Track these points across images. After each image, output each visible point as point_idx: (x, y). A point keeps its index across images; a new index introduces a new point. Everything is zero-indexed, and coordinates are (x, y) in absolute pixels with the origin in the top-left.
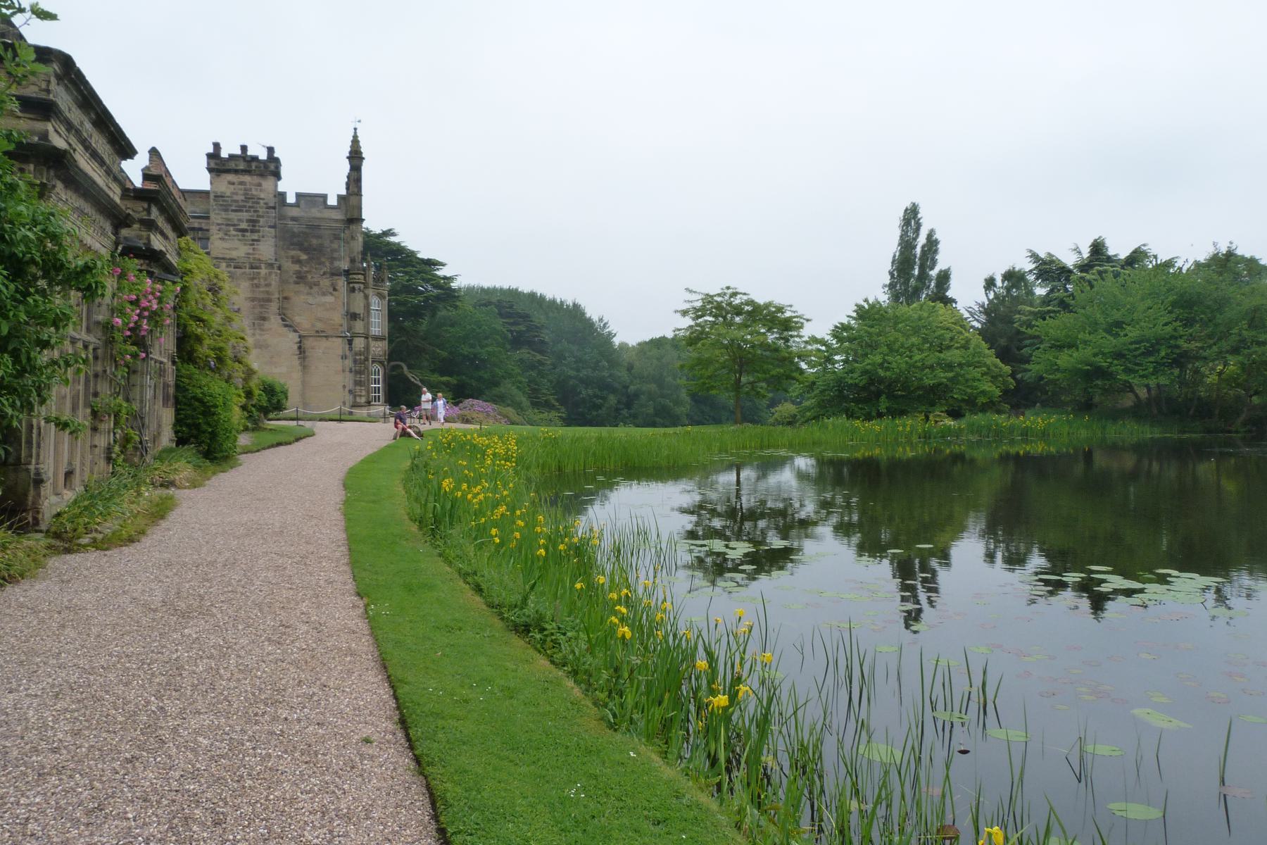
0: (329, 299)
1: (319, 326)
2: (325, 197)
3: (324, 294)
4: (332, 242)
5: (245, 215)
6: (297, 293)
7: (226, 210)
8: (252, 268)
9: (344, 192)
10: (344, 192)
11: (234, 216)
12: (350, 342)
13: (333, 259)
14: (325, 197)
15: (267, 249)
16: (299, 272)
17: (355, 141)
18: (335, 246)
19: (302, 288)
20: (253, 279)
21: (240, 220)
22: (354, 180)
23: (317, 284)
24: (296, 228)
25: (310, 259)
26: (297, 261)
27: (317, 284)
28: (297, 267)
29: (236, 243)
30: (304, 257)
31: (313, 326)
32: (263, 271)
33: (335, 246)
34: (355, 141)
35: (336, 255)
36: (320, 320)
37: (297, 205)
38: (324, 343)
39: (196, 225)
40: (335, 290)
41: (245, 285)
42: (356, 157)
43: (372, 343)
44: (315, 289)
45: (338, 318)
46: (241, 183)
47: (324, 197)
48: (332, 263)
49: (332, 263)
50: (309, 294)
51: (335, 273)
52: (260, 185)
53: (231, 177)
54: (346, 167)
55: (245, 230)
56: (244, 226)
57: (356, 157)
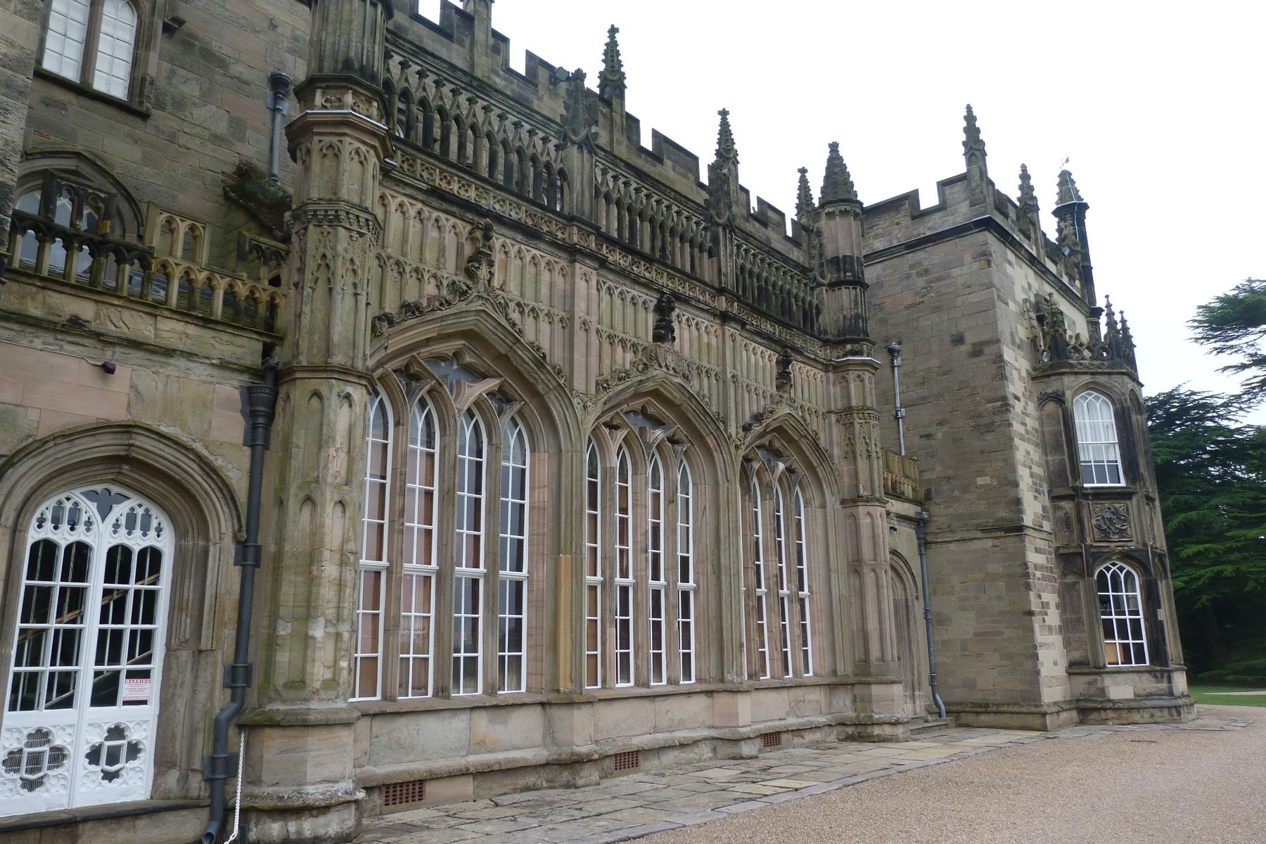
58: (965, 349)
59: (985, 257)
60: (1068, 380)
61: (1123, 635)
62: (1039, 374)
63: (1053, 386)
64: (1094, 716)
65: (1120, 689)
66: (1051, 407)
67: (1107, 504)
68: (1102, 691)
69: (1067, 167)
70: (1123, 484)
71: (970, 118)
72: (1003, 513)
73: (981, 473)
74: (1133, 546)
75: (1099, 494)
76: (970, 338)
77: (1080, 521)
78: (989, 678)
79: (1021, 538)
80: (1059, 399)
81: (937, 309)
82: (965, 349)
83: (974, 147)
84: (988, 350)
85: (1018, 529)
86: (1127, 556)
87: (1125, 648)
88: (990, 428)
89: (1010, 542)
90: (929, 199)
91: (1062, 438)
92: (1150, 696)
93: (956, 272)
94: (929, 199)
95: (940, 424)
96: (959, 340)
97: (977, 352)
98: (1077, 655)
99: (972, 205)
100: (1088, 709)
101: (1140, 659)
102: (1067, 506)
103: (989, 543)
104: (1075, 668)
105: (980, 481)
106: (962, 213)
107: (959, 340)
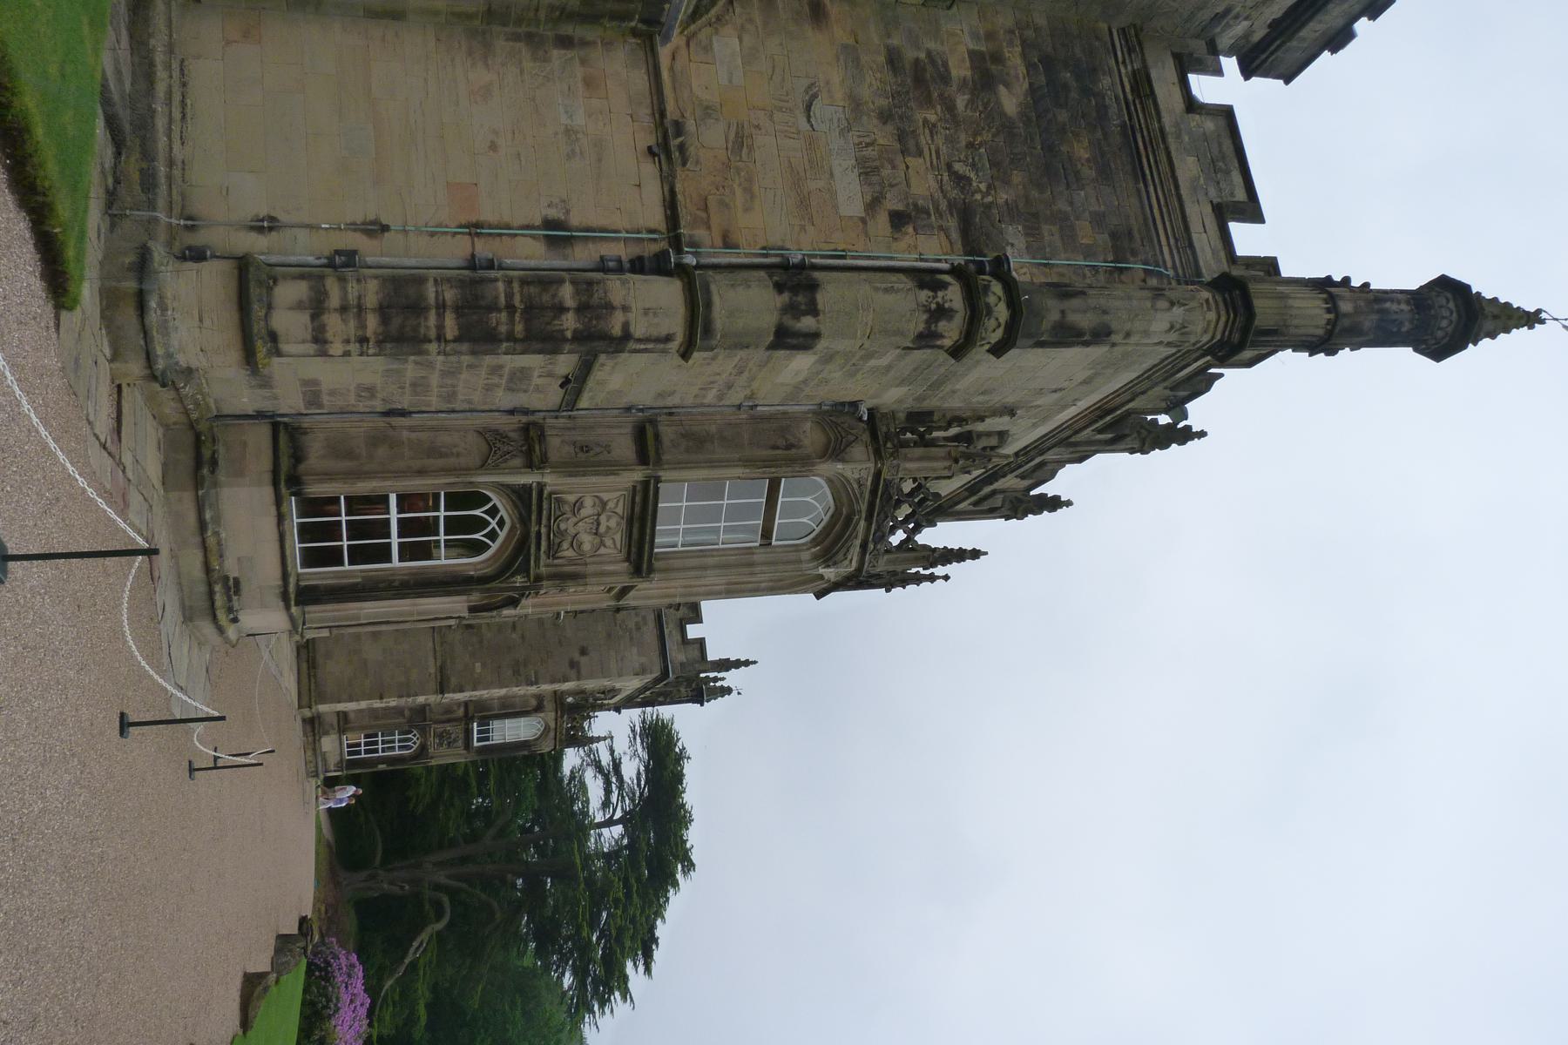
0: (850, 195)
1: (709, 140)
2: (1252, 212)
3: (867, 171)
4: (1098, 220)
6: (850, 55)
12: (658, 266)
13: (1032, 222)
14: (1252, 212)
16: (945, 78)
18: (1085, 233)
19: (874, 85)
22: (1346, 317)
23: (906, 142)
24: (1112, 83)
25: (1007, 127)
26: (986, 73)
27: (906, 142)
28: (960, 69)
30: (1010, 102)
31: (708, 111)
33: (1085, 233)
35: (1050, 232)
36: (740, 141)
37: (1192, 105)
38: (627, 137)
40: (899, 220)
43: (615, 489)
44: (884, 136)
45: (767, 223)
48: (1012, 212)
49: (1012, 212)
50: (856, 104)
51: (970, 224)
58: (576, 656)
59: (642, 671)
60: (552, 715)
61: (366, 744)
62: (558, 697)
63: (549, 704)
64: (309, 728)
65: (328, 744)
66: (534, 702)
67: (462, 736)
68: (326, 733)
69: (735, 693)
70: (476, 744)
71: (747, 663)
72: (454, 681)
73: (484, 665)
74: (431, 750)
75: (468, 733)
76: (583, 660)
77: (449, 721)
78: (334, 669)
79: (436, 693)
80: (539, 708)
81: (609, 635)
82: (576, 656)
83: (726, 665)
84: (573, 673)
85: (442, 690)
86: (423, 748)
87: (359, 745)
88: (516, 672)
89: (433, 685)
90: (693, 631)
91: (511, 710)
92: (325, 760)
93: (635, 650)
94: (693, 631)
95: (523, 637)
96: (583, 652)
97: (573, 665)
98: (352, 716)
99: (682, 664)
100: (314, 726)
101: (350, 753)
102: (461, 712)
103: (432, 671)
104: (343, 717)
105: (478, 665)
106: (677, 655)
107: (583, 652)
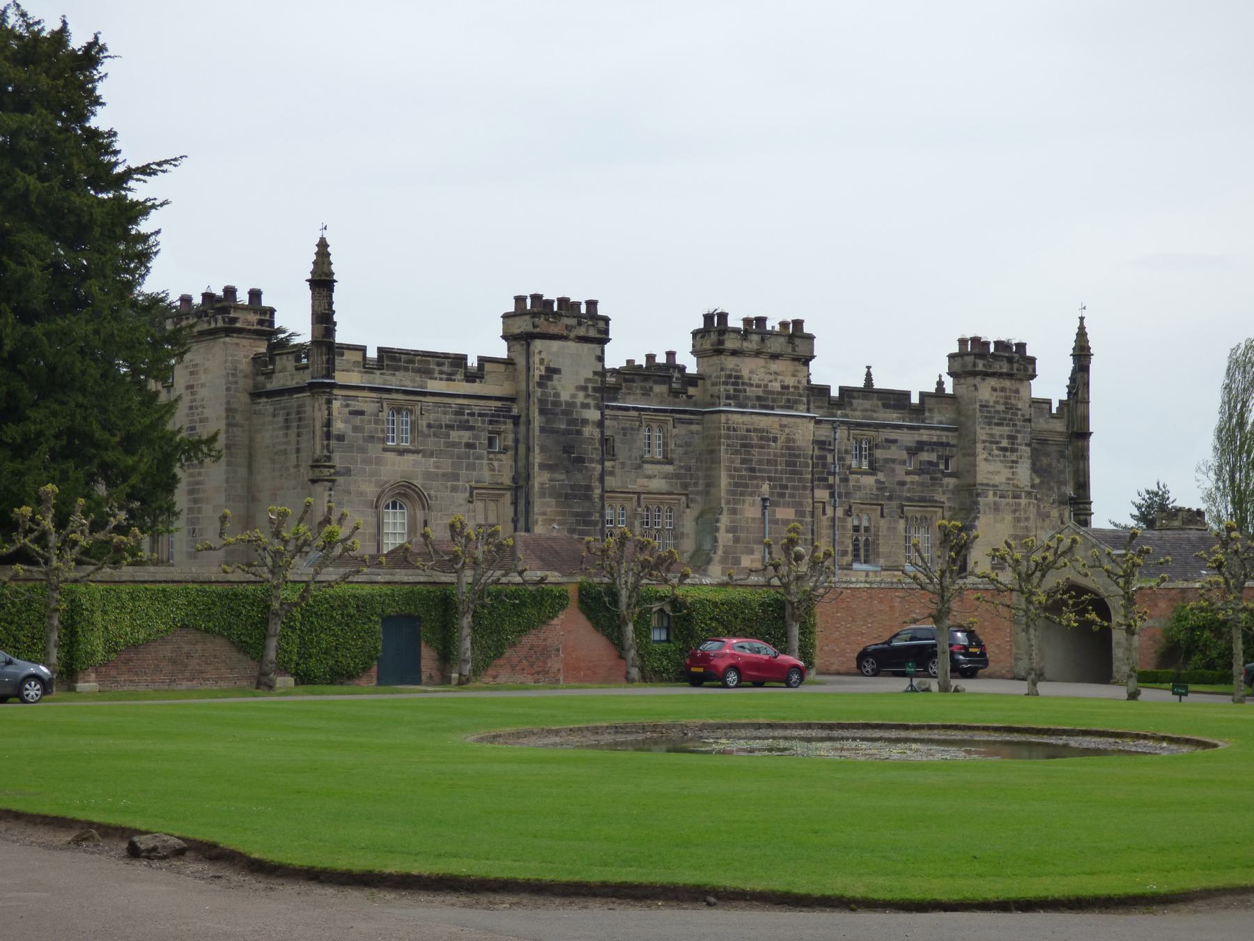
5: (1005, 430)
7: (989, 424)
8: (1014, 497)
9: (1065, 397)
10: (1065, 397)
11: (997, 430)
15: (1024, 474)
17: (1082, 334)
20: (1015, 511)
21: (1001, 436)
29: (998, 466)
32: (1023, 501)
34: (1082, 334)
39: (944, 440)
41: (1009, 518)
42: (1082, 354)
46: (1003, 390)
47: (1048, 402)
52: (1017, 392)
53: (993, 382)
54: (1069, 365)
55: (1004, 449)
56: (1005, 443)
57: (1082, 354)
